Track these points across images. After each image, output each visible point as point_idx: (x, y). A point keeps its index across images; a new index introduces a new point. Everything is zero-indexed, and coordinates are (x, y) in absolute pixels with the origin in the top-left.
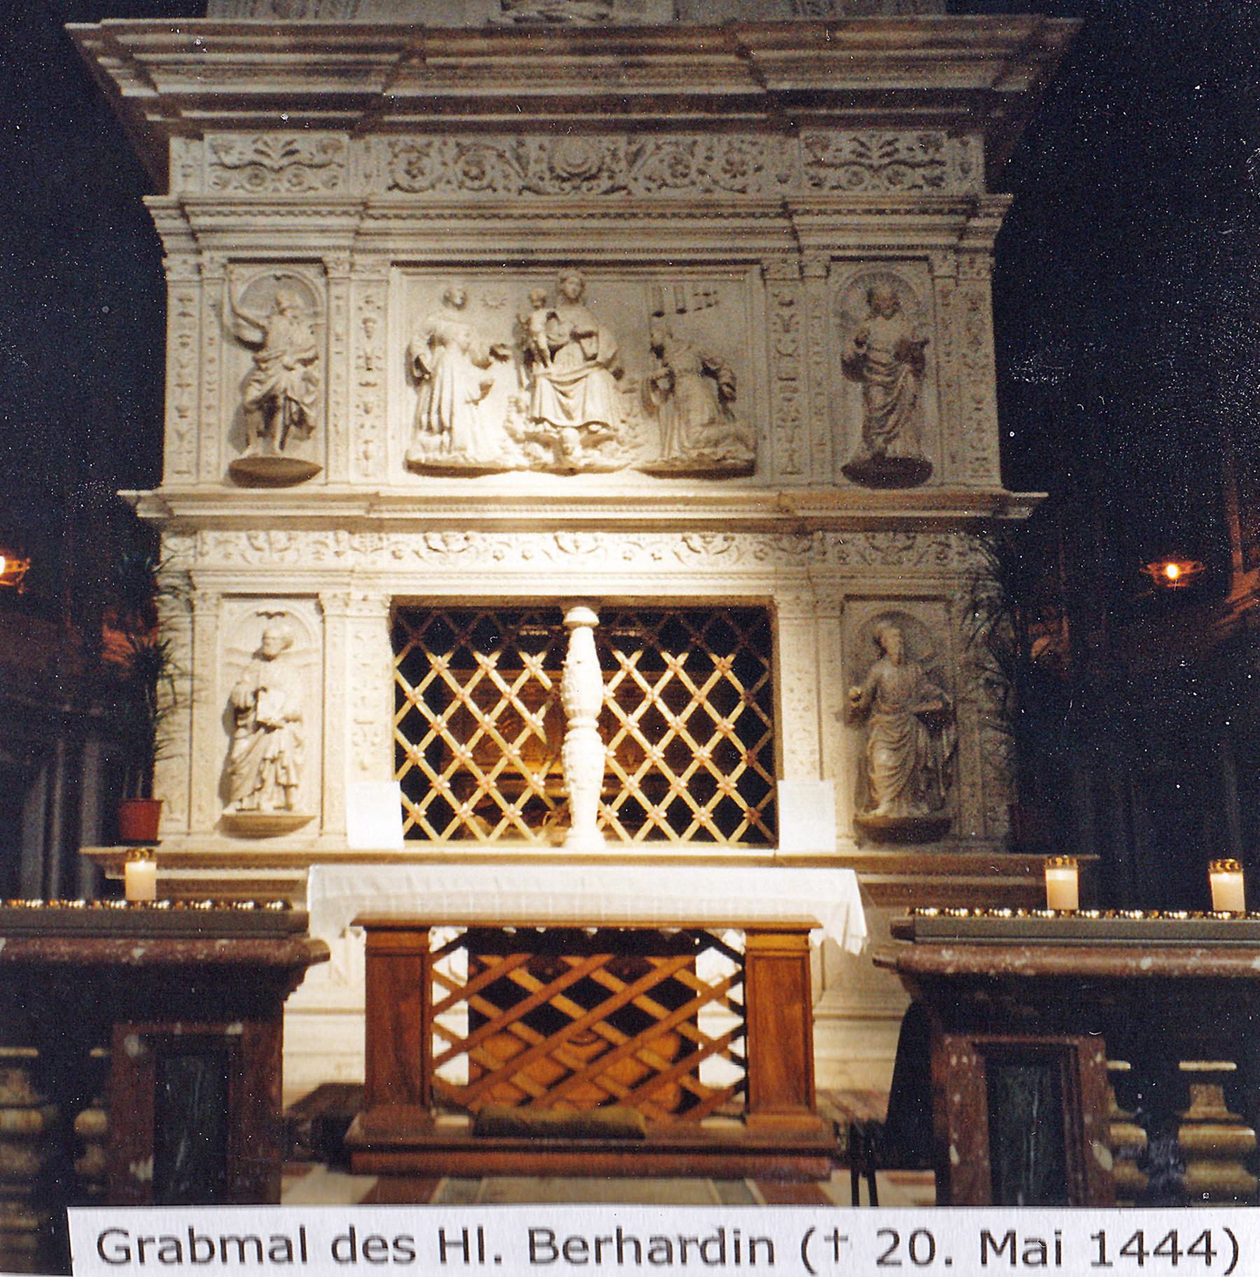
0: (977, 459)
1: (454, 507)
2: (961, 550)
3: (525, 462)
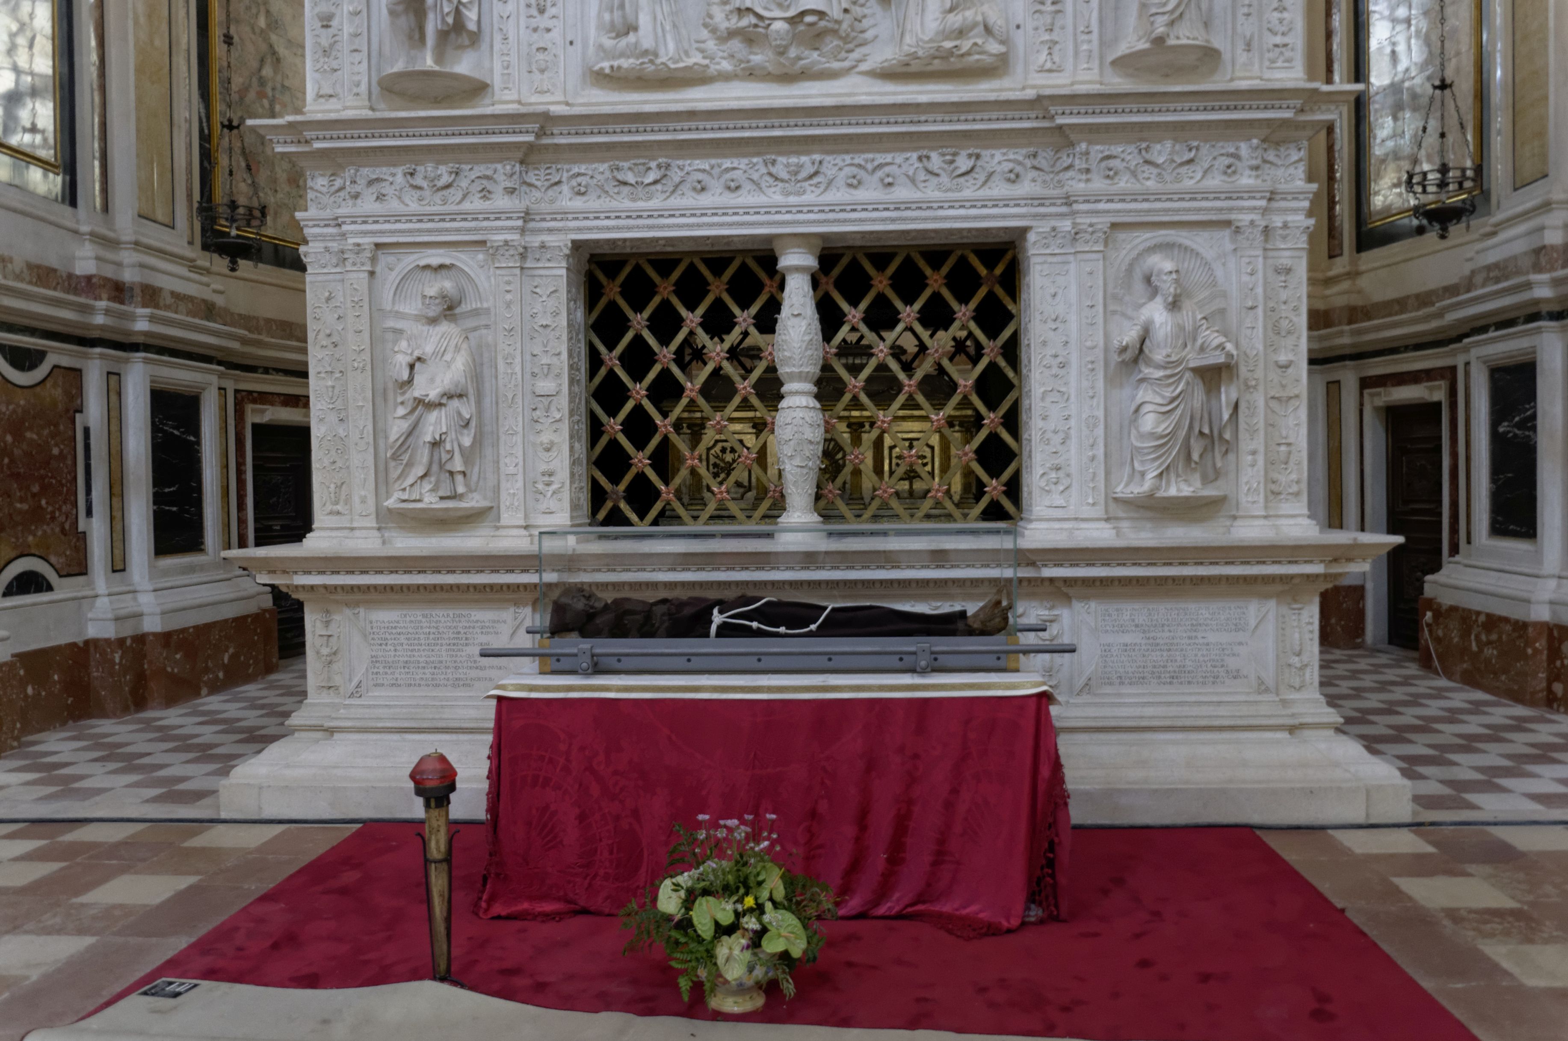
0: (1276, 46)
1: (641, 127)
2: (1254, 162)
3: (726, 66)
